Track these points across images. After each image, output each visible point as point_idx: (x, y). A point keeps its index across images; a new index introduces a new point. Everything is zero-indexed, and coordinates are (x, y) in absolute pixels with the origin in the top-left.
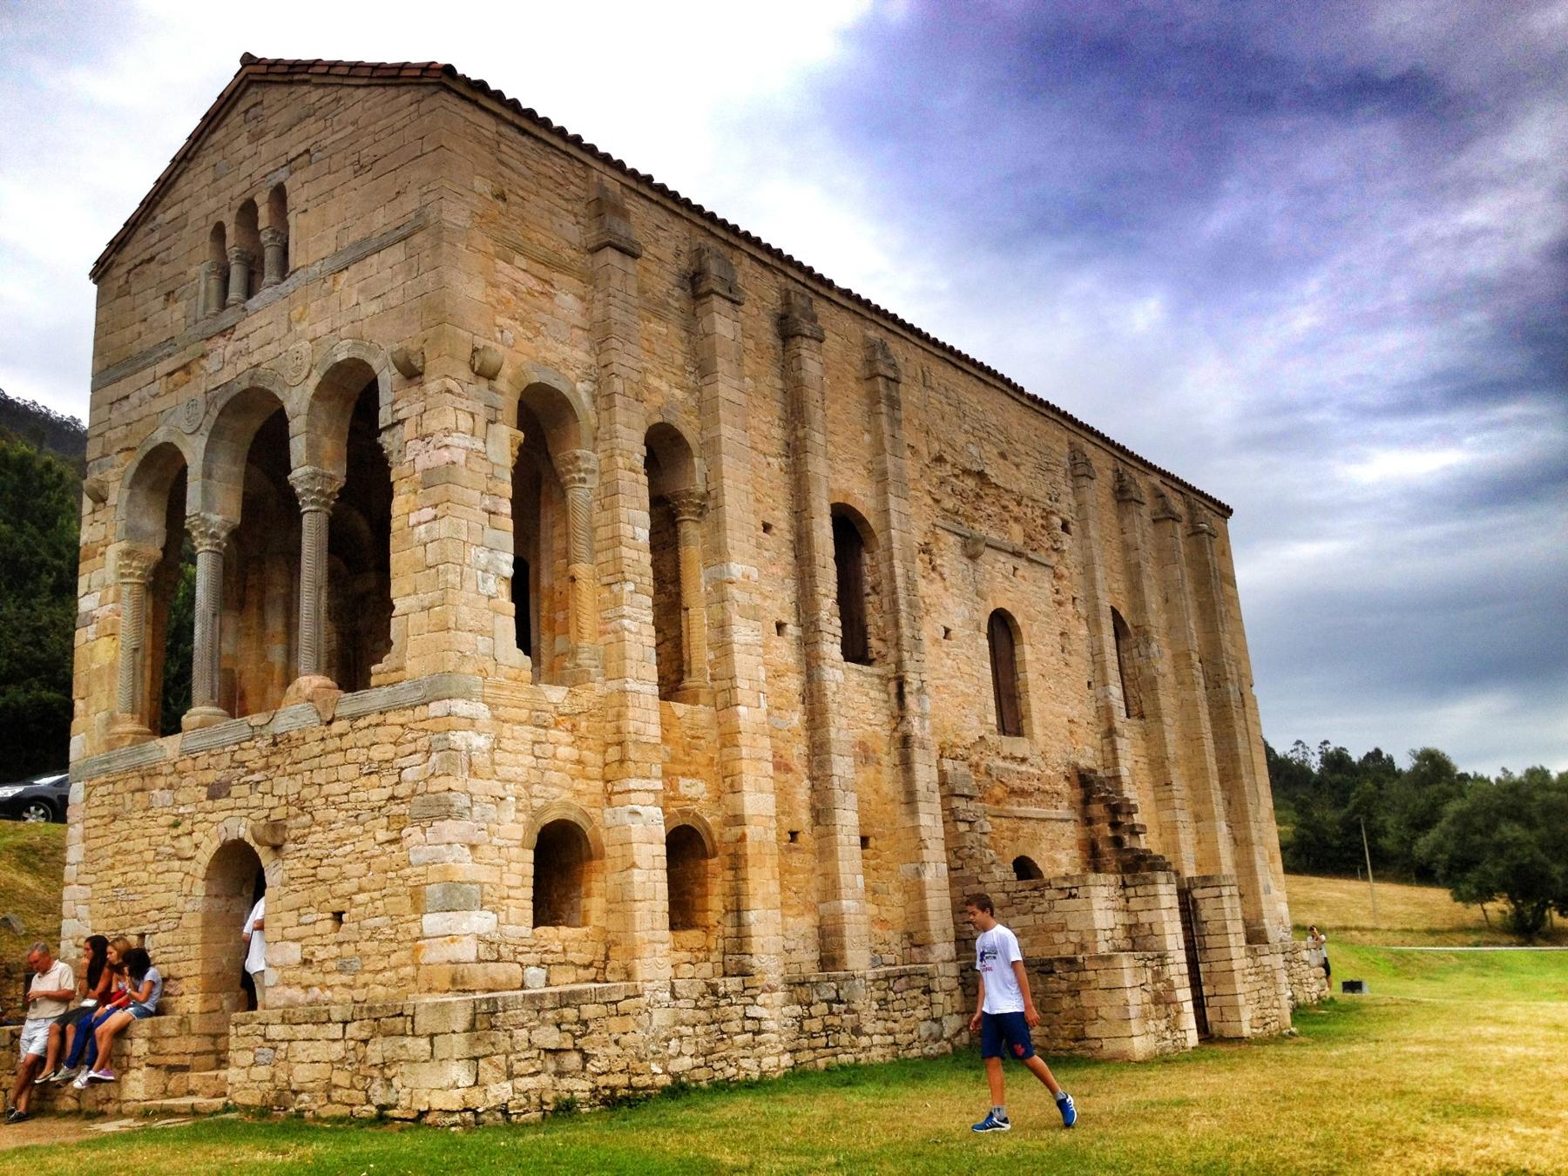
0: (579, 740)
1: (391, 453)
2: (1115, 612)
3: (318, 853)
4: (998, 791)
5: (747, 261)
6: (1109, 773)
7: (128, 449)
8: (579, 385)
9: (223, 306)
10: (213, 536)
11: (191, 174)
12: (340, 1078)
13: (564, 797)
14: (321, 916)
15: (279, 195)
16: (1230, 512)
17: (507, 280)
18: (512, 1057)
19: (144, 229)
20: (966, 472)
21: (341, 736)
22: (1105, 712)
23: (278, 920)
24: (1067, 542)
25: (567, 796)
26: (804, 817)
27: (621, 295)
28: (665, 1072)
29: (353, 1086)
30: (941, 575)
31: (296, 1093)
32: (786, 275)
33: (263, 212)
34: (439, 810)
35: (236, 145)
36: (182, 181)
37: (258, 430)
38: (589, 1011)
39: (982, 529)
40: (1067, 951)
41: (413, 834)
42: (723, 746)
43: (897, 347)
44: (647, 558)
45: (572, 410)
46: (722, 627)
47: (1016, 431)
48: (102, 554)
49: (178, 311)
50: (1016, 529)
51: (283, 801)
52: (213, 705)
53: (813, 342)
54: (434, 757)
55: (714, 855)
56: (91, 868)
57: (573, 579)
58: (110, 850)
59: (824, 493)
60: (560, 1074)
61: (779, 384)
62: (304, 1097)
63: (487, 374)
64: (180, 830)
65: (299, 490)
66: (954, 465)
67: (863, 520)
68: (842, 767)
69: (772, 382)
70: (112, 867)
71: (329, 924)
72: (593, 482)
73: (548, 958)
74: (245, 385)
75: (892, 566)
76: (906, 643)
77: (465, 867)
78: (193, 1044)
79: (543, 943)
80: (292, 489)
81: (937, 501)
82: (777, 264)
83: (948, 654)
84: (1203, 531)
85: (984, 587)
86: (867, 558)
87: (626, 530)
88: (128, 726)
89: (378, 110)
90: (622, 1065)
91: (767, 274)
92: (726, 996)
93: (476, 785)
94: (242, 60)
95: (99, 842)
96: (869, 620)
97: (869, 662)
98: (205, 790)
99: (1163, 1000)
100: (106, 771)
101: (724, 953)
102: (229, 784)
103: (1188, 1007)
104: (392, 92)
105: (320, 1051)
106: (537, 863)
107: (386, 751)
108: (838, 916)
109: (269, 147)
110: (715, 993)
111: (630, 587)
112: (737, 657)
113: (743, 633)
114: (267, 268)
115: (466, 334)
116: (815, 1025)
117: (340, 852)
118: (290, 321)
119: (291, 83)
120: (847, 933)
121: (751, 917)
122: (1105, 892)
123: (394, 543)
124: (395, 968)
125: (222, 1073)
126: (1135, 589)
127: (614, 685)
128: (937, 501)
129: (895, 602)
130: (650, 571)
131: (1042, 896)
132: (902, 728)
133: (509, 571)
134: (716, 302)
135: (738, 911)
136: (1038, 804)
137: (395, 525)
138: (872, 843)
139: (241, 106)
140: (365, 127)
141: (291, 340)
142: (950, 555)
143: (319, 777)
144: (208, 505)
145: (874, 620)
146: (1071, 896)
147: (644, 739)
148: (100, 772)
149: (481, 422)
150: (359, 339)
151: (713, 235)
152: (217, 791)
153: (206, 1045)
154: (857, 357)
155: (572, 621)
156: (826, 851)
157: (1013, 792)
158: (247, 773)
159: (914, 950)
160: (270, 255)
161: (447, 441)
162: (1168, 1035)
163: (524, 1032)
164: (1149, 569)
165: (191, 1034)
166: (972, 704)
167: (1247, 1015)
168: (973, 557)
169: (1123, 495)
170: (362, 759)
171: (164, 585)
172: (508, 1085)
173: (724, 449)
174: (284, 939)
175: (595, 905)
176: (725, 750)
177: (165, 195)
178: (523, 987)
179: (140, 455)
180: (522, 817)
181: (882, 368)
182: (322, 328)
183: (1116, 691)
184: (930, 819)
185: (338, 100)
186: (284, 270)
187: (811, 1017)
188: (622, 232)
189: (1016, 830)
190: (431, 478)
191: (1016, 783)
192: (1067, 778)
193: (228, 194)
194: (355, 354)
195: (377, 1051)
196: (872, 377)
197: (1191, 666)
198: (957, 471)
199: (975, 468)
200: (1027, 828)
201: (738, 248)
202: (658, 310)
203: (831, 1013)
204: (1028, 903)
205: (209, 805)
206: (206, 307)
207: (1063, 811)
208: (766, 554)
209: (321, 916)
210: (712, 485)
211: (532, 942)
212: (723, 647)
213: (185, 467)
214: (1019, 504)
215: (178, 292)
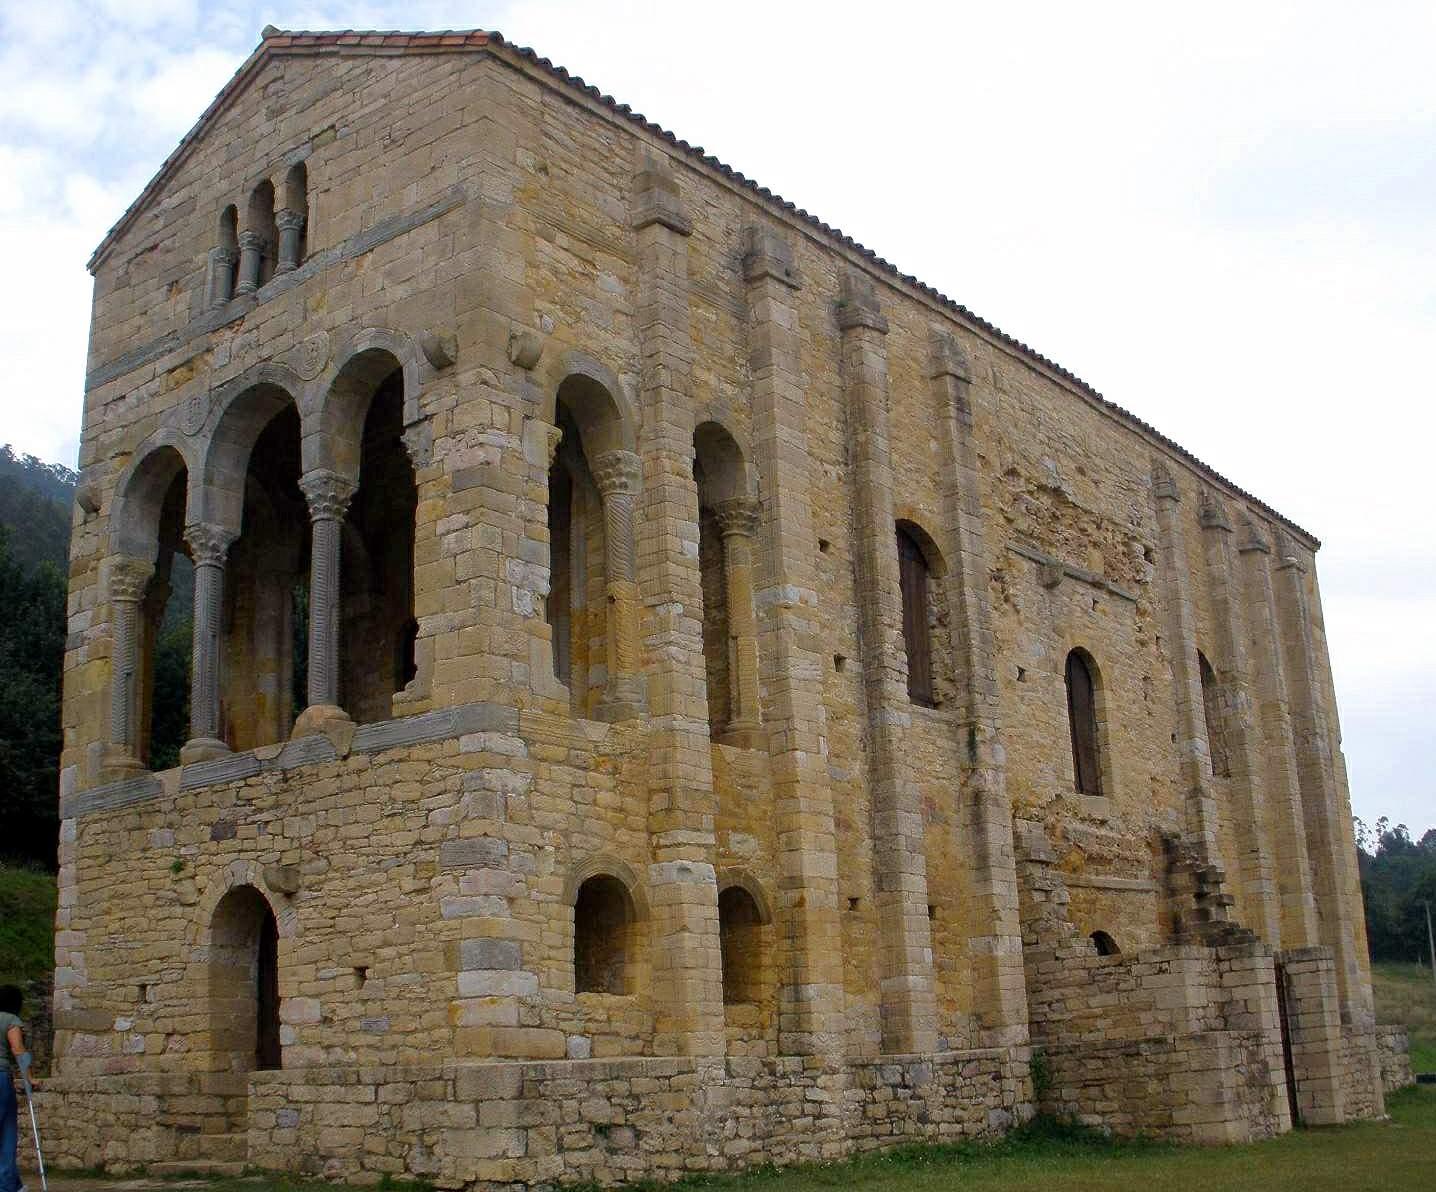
0: (621, 786)
1: (415, 453)
2: (1201, 656)
4: (1075, 858)
5: (802, 242)
6: (1193, 838)
7: (124, 454)
8: (621, 377)
9: (232, 294)
10: (215, 548)
11: (201, 156)
12: (372, 1143)
13: (609, 849)
14: (341, 971)
15: (300, 173)
16: (1318, 545)
17: (546, 260)
18: (562, 1129)
19: (150, 214)
20: (1042, 488)
21: (359, 772)
22: (1191, 769)
23: (294, 974)
24: (1150, 573)
25: (609, 847)
26: (866, 882)
27: (668, 277)
28: (722, 1154)
29: (391, 1154)
30: (1014, 606)
31: (323, 1158)
32: (846, 259)
33: (280, 192)
34: (473, 856)
35: (254, 121)
36: (192, 163)
37: (267, 430)
38: (642, 1085)
39: (1059, 555)
40: (1154, 1032)
41: (444, 883)
42: (778, 797)
43: (965, 343)
44: (696, 576)
45: (612, 405)
46: (778, 659)
47: (1097, 444)
48: (94, 569)
49: (181, 303)
50: (1096, 555)
51: (296, 844)
52: (214, 737)
53: (876, 334)
54: (467, 797)
55: (769, 922)
56: (85, 912)
57: (612, 600)
58: (106, 893)
59: (888, 507)
60: (612, 1151)
61: (837, 381)
62: (335, 1162)
63: (525, 363)
64: (182, 874)
65: (310, 496)
66: (1028, 480)
67: (929, 541)
68: (910, 825)
69: (830, 377)
70: (108, 912)
71: (352, 980)
72: (637, 487)
73: (592, 1026)
74: (254, 381)
75: (962, 594)
76: (977, 683)
77: (503, 921)
78: (202, 1104)
79: (585, 1010)
80: (303, 495)
81: (1009, 521)
82: (836, 246)
83: (1022, 698)
84: (1291, 566)
85: (1061, 622)
86: (932, 584)
87: (673, 543)
88: (123, 758)
89: (414, 82)
90: (673, 1144)
91: (825, 257)
92: (784, 1076)
93: (511, 831)
94: (263, 34)
95: (94, 885)
96: (934, 656)
97: (936, 706)
98: (209, 830)
99: (1258, 1081)
101: (780, 1030)
102: (234, 824)
103: (1282, 1090)
104: (429, 62)
105: (349, 1114)
106: (579, 921)
107: (412, 790)
108: (904, 995)
109: (287, 125)
110: (772, 1073)
111: (678, 609)
112: (794, 694)
113: (802, 667)
114: (281, 253)
115: (502, 319)
116: (879, 1111)
118: (306, 310)
119: (317, 55)
120: (914, 1010)
121: (810, 991)
122: (1197, 966)
123: (418, 553)
125: (237, 1137)
126: (1222, 629)
127: (659, 722)
128: (1009, 521)
129: (966, 637)
130: (699, 590)
131: (1129, 972)
132: (973, 782)
133: (545, 588)
134: (772, 287)
135: (796, 984)
136: (1117, 873)
137: (419, 534)
138: (938, 913)
139: (260, 81)
140: (398, 100)
141: (305, 334)
142: (1024, 585)
143: (335, 818)
144: (208, 516)
145: (941, 656)
146: (1161, 971)
147: (694, 785)
149: (517, 415)
150: (383, 328)
151: (767, 213)
152: (222, 831)
153: (216, 1105)
154: (922, 352)
155: (611, 648)
156: (890, 921)
157: (1091, 859)
158: (255, 812)
159: (983, 1033)
160: (286, 239)
161: (482, 438)
162: (1261, 1120)
163: (574, 1103)
164: (1236, 607)
165: (200, 1093)
166: (1048, 757)
167: (1341, 1099)
168: (1051, 586)
169: (1208, 522)
171: (155, 600)
172: (559, 1159)
173: (779, 453)
175: (639, 972)
176: (780, 803)
177: (171, 178)
178: (566, 1056)
179: (137, 460)
180: (562, 870)
181: (951, 367)
182: (341, 316)
183: (1202, 744)
184: (1004, 888)
185: (369, 72)
186: (300, 255)
187: (874, 1102)
188: (672, 208)
189: (1093, 902)
190: (461, 481)
191: (1095, 849)
192: (1149, 844)
194: (379, 344)
195: (413, 1116)
196: (938, 376)
197: (1280, 718)
198: (1032, 487)
199: (1051, 484)
200: (1105, 900)
201: (793, 227)
202: (705, 293)
203: (896, 1098)
204: (1112, 980)
205: (213, 846)
206: (213, 295)
207: (1143, 879)
208: (824, 576)
209: (341, 971)
210: (766, 494)
211: (575, 1008)
212: (778, 682)
213: (184, 472)
214: (1099, 527)
215: (182, 282)
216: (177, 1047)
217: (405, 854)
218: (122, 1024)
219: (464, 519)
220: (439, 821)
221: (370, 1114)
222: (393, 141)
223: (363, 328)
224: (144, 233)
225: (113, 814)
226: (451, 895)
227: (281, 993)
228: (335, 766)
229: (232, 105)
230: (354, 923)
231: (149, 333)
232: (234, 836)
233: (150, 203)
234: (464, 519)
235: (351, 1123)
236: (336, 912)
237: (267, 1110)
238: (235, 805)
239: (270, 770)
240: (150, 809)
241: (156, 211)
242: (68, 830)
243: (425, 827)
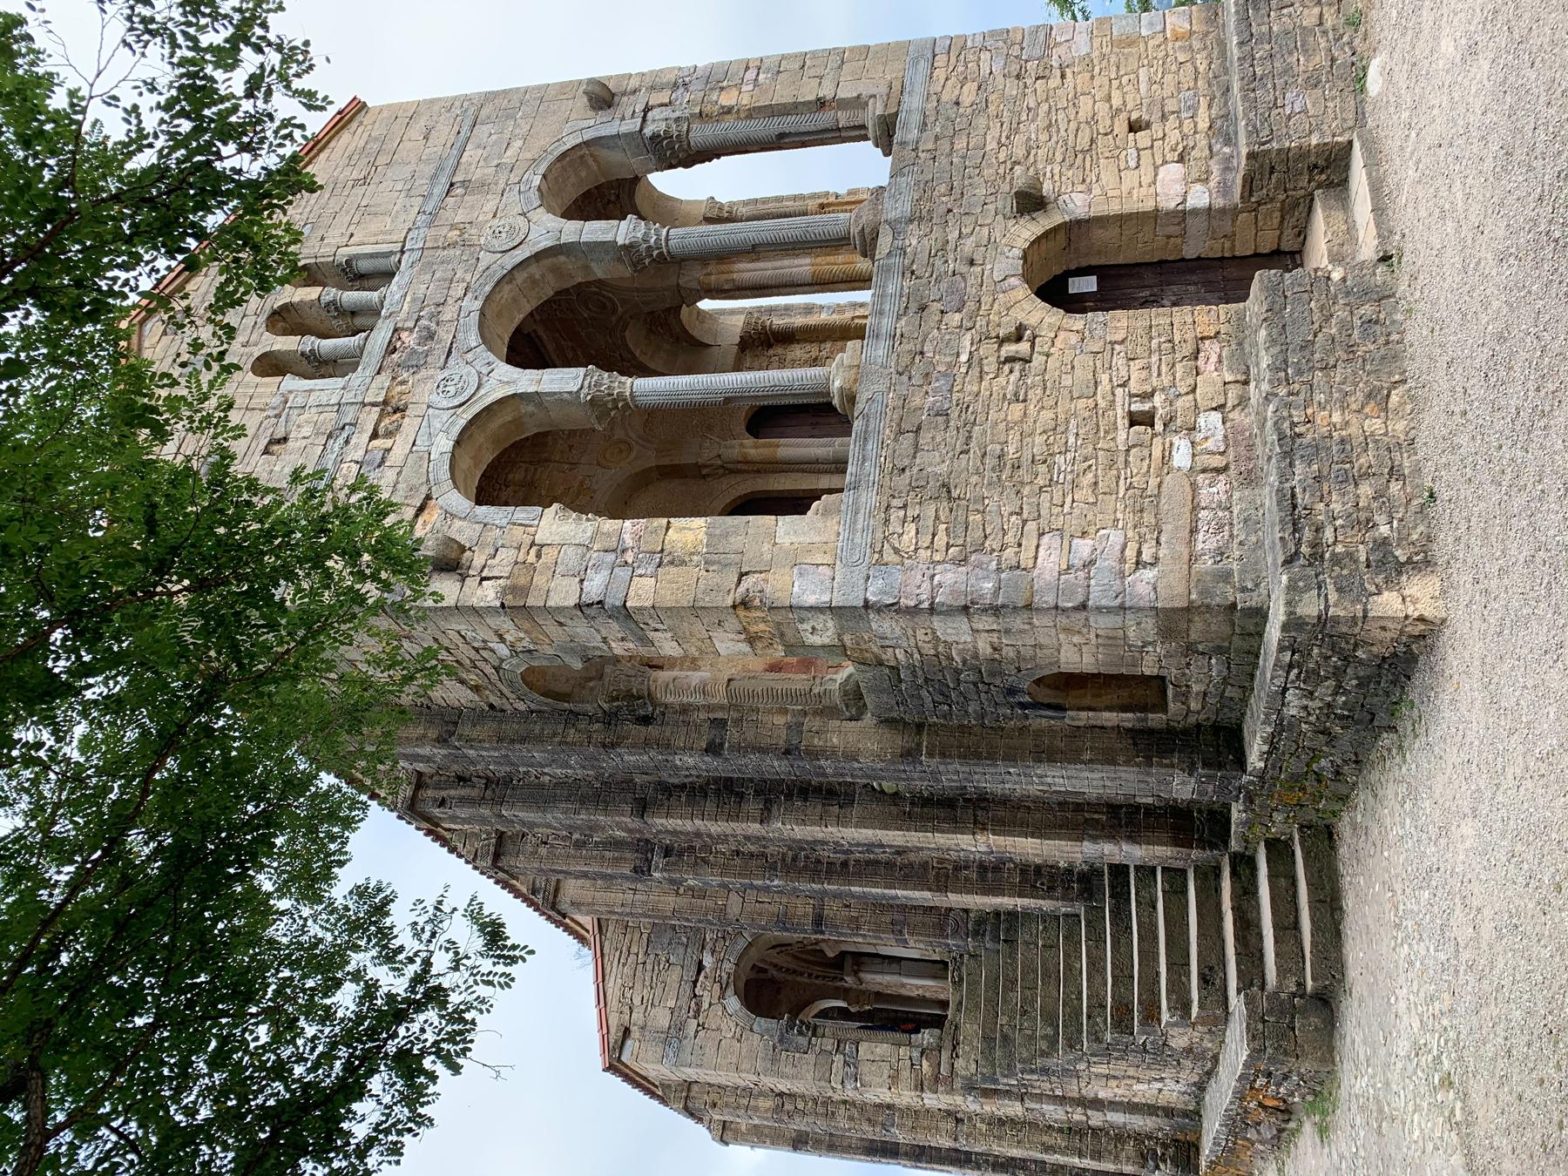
117: (1062, 127)
216: (1214, 358)
218: (1182, 457)
227: (1149, 206)
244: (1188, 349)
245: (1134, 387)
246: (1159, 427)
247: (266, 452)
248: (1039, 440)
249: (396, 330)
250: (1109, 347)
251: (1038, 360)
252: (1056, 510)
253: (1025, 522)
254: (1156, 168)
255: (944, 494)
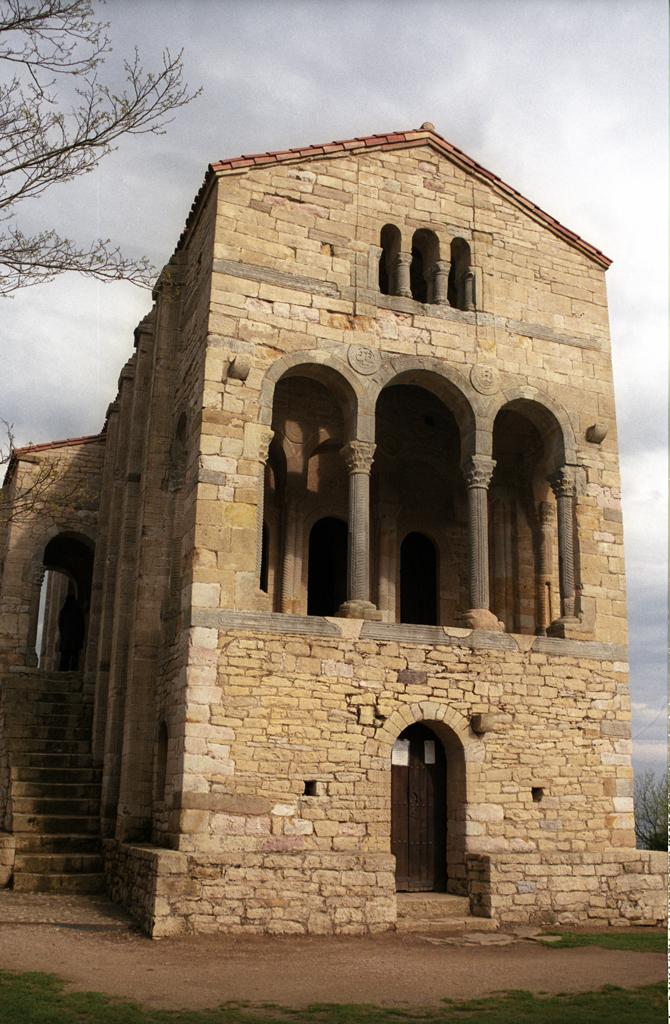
3: (522, 744)
7: (275, 349)
12: (595, 901)
14: (523, 789)
21: (540, 666)
23: (483, 787)
29: (609, 907)
36: (343, 164)
41: (604, 745)
74: (429, 367)
100: (252, 628)
104: (563, 245)
107: (576, 685)
117: (541, 746)
124: (594, 830)
140: (545, 254)
148: (243, 627)
152: (406, 677)
158: (443, 671)
170: (560, 685)
174: (487, 801)
182: (511, 367)
185: (517, 218)
193: (404, 211)
205: (400, 687)
216: (351, 832)
217: (577, 722)
218: (280, 810)
219: (612, 539)
220: (600, 707)
221: (593, 883)
222: (541, 277)
223: (528, 384)
224: (285, 183)
225: (273, 638)
226: (609, 751)
227: (470, 797)
228: (519, 658)
229: (387, 151)
230: (536, 760)
231: (300, 269)
232: (425, 683)
233: (291, 164)
234: (612, 539)
235: (580, 888)
236: (520, 751)
237: (509, 881)
238: (425, 662)
239: (459, 647)
240: (325, 644)
241: (295, 173)
242: (203, 637)
243: (589, 708)
244: (358, 816)
245: (334, 786)
246: (306, 798)
247: (324, 244)
248: (300, 729)
249: (412, 314)
250: (364, 771)
251: (359, 728)
252: (250, 738)
253: (243, 720)
254: (501, 804)
255: (265, 673)
